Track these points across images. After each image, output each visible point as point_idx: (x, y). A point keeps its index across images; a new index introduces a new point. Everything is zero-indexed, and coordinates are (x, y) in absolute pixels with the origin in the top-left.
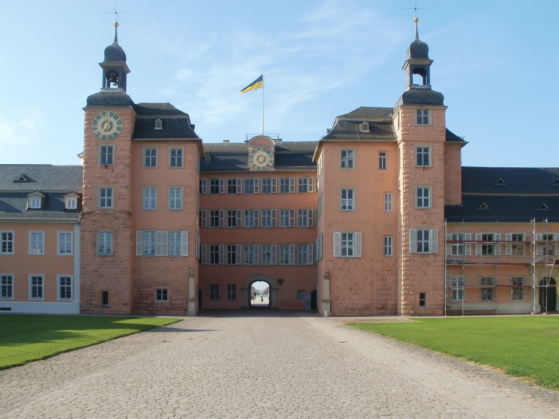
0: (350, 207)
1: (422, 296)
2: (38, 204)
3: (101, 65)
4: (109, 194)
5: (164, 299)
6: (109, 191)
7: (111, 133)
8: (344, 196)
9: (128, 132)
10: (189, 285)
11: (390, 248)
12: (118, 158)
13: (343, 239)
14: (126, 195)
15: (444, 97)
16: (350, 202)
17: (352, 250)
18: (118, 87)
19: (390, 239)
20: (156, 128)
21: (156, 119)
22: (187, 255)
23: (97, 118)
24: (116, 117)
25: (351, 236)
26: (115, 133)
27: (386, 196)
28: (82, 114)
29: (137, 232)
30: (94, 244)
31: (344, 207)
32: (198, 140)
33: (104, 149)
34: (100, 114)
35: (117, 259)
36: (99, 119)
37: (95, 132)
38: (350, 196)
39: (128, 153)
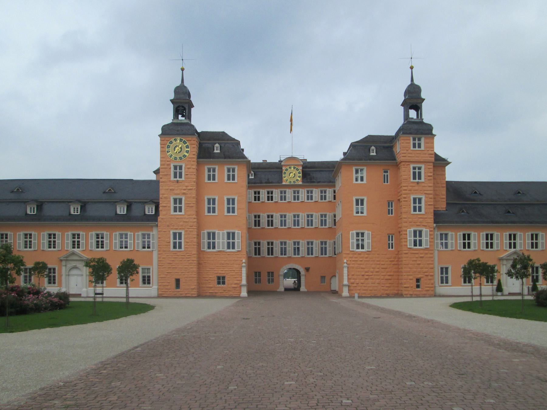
0: (362, 213)
1: (418, 280)
2: (124, 210)
3: (172, 101)
4: (180, 203)
5: (222, 284)
6: (180, 200)
7: (181, 155)
8: (357, 204)
9: (194, 155)
10: (242, 273)
11: (392, 243)
13: (357, 237)
14: (194, 204)
15: (433, 128)
16: (362, 209)
17: (364, 246)
18: (185, 119)
19: (392, 237)
20: (215, 151)
21: (216, 143)
22: (240, 250)
23: (170, 143)
25: (363, 234)
27: (389, 203)
29: (202, 232)
30: (169, 241)
31: (357, 213)
32: (247, 161)
33: (175, 168)
34: (173, 140)
35: (187, 253)
36: (171, 144)
37: (168, 154)
38: (362, 204)
39: (195, 170)
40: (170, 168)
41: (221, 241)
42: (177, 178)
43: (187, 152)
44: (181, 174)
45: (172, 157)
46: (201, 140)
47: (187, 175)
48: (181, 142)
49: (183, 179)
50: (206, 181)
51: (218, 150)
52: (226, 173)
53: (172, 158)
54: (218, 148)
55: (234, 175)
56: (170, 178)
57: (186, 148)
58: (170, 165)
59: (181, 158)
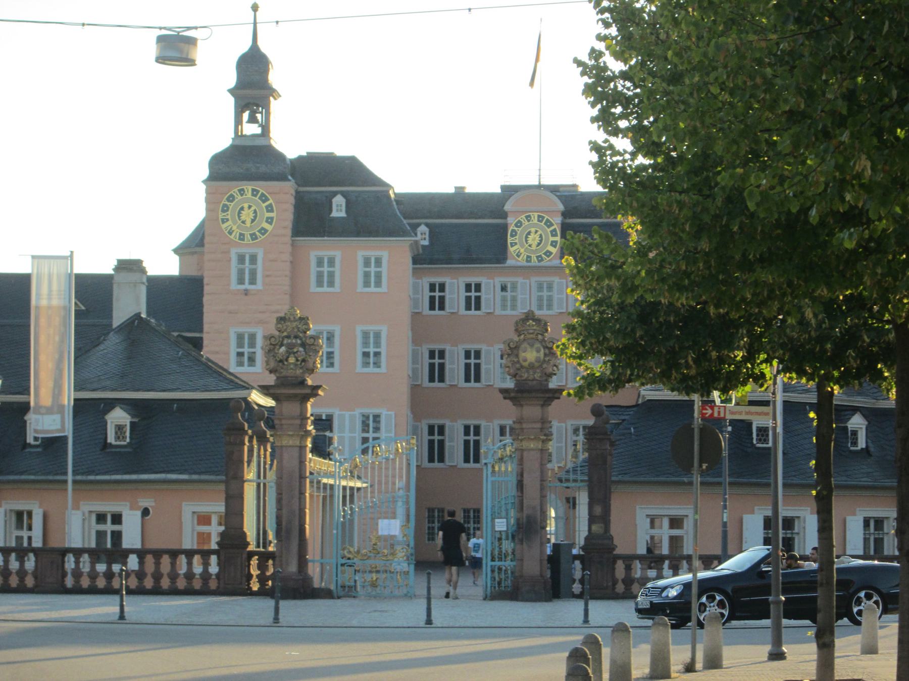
3: (231, 91)
9: (285, 228)
12: (268, 276)
20: (335, 214)
21: (335, 194)
23: (228, 200)
24: (264, 199)
26: (263, 228)
28: (200, 192)
33: (241, 259)
36: (232, 201)
37: (224, 226)
40: (229, 260)
41: (347, 434)
42: (244, 284)
43: (270, 221)
44: (253, 274)
45: (234, 234)
46: (299, 185)
47: (268, 276)
48: (255, 196)
49: (259, 286)
50: (314, 288)
51: (341, 211)
52: (361, 269)
53: (232, 237)
54: (341, 206)
55: (380, 272)
56: (229, 285)
57: (268, 211)
58: (228, 252)
59: (254, 237)
